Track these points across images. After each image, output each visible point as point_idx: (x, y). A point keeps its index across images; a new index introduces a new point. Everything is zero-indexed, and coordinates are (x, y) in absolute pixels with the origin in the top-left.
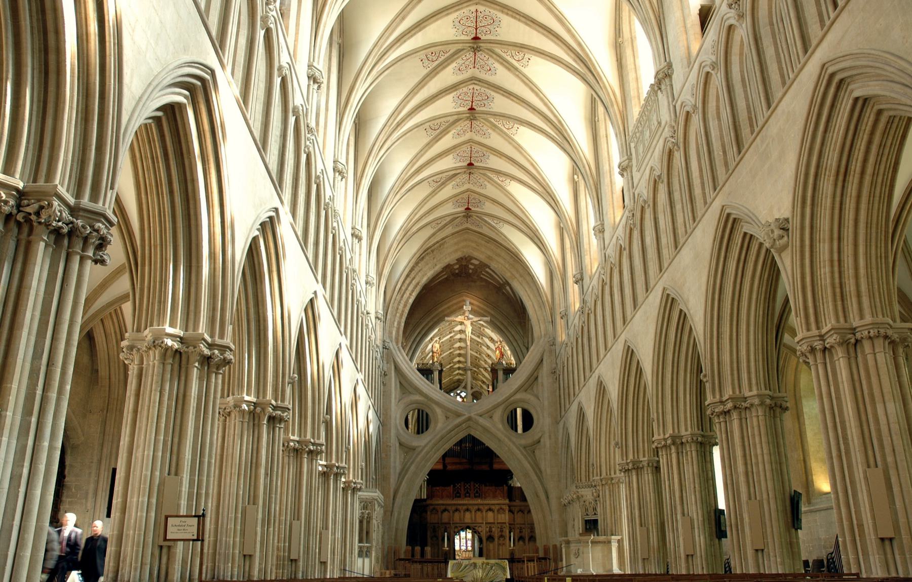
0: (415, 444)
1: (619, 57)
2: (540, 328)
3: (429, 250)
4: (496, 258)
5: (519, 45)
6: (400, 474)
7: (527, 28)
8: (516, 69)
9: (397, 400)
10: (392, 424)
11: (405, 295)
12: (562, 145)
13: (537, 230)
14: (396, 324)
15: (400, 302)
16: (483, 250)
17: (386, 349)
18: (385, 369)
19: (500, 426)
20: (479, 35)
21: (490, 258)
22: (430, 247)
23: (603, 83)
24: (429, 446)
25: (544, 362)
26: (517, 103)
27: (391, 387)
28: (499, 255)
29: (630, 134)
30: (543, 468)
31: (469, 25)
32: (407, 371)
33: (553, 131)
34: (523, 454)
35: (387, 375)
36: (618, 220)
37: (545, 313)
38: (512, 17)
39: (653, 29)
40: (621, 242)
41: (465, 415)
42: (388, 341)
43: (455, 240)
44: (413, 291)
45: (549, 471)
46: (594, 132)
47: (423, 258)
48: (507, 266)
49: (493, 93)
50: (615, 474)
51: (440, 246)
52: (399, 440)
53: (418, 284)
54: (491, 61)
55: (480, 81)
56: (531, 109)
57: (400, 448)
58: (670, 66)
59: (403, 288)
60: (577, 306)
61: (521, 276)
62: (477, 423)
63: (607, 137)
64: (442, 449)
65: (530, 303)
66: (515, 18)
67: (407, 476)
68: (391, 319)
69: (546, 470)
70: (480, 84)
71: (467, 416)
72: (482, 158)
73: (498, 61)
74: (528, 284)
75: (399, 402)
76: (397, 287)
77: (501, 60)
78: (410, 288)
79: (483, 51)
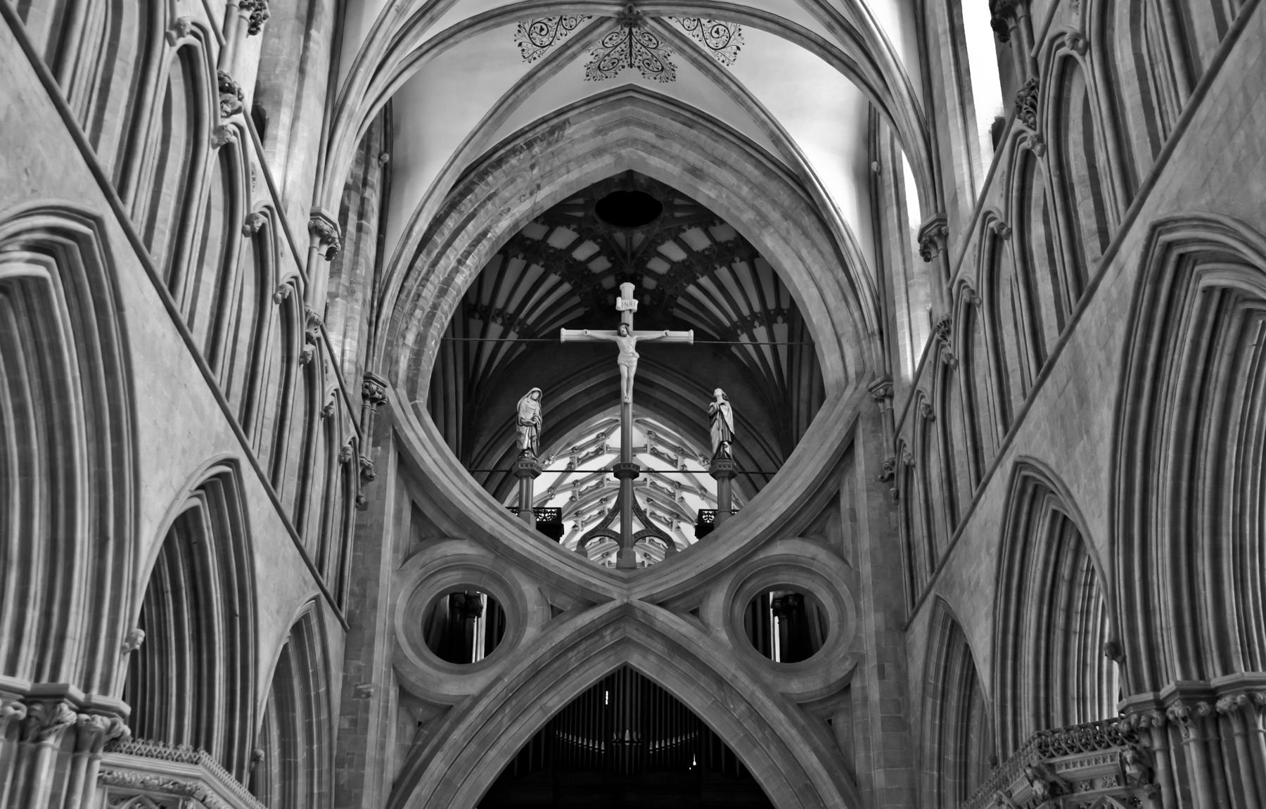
2: (843, 358)
3: (520, 141)
4: (713, 169)
6: (396, 785)
9: (401, 557)
11: (442, 262)
14: (410, 338)
15: (426, 279)
16: (676, 148)
17: (373, 400)
18: (367, 455)
19: (724, 636)
21: (695, 172)
22: (522, 133)
24: (493, 694)
25: (860, 451)
27: (382, 513)
28: (721, 163)
30: (860, 768)
34: (794, 723)
35: (371, 478)
37: (857, 315)
41: (614, 599)
42: (381, 378)
43: (596, 118)
44: (467, 254)
45: (879, 778)
47: (500, 162)
48: (745, 190)
50: (1227, 669)
51: (552, 131)
53: (484, 234)
59: (439, 240)
61: (786, 216)
62: (650, 628)
64: (537, 707)
65: (814, 291)
67: (417, 790)
68: (393, 320)
69: (870, 779)
71: (617, 603)
76: (416, 229)
78: (462, 243)
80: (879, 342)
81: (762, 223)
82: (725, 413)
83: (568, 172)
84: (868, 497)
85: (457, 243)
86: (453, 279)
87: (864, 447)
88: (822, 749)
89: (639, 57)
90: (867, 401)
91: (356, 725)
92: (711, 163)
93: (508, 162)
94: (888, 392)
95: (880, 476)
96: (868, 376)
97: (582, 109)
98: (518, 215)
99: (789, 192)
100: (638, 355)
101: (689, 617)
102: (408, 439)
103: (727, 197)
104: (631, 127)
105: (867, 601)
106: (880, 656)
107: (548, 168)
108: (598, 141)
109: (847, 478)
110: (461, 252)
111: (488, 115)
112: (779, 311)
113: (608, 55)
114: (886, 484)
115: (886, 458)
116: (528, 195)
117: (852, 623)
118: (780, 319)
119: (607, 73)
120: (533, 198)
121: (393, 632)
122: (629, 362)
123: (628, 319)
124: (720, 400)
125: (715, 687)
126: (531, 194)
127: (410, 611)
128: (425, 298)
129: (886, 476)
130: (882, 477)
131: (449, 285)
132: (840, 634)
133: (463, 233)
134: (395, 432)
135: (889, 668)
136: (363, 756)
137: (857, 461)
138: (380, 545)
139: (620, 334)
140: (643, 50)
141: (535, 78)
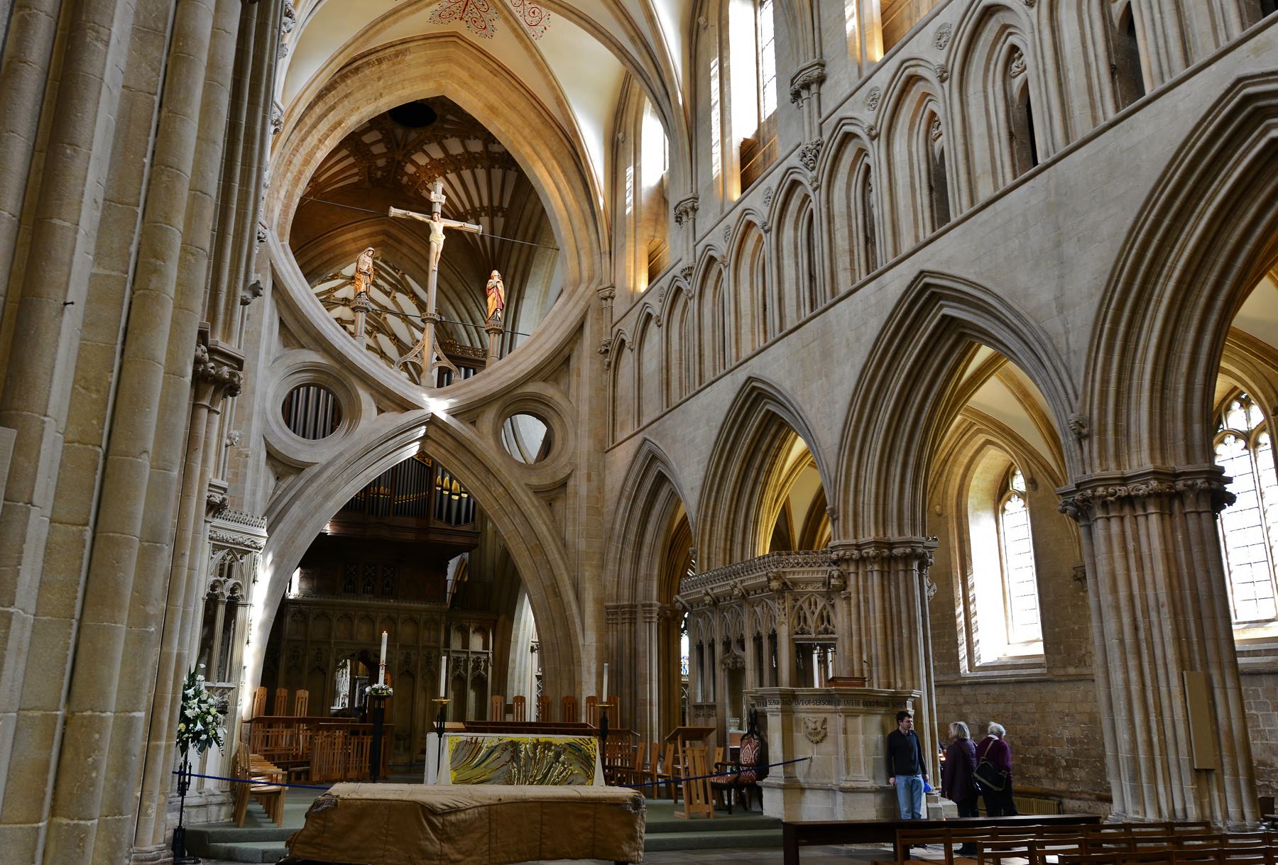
0: (304, 457)
3: (373, 57)
4: (507, 111)
10: (256, 408)
11: (309, 139)
14: (283, 193)
15: (296, 150)
16: (482, 89)
21: (492, 109)
22: (375, 51)
27: (261, 324)
30: (569, 536)
32: (299, 296)
37: (594, 237)
43: (428, 52)
44: (326, 136)
45: (582, 545)
47: (357, 70)
48: (527, 131)
51: (396, 56)
52: (268, 445)
53: (339, 123)
57: (267, 464)
59: (309, 121)
67: (281, 526)
75: (273, 362)
78: (323, 127)
80: (608, 259)
82: (500, 288)
83: (403, 88)
84: (591, 362)
85: (320, 126)
86: (315, 154)
88: (548, 522)
89: (470, 15)
90: (595, 297)
91: (237, 476)
93: (362, 72)
96: (596, 281)
97: (420, 43)
98: (364, 114)
99: (558, 140)
100: (444, 237)
101: (470, 426)
102: (281, 272)
103: (513, 133)
104: (452, 65)
105: (584, 430)
106: (589, 467)
107: (390, 83)
108: (426, 70)
109: (577, 346)
110: (321, 133)
111: (359, 34)
112: (500, 208)
113: (449, 8)
116: (373, 100)
117: (571, 443)
118: (500, 214)
119: (445, 21)
120: (376, 103)
121: (263, 413)
122: (438, 240)
123: (438, 208)
124: (496, 279)
125: (483, 475)
126: (376, 100)
127: (276, 397)
128: (295, 165)
129: (603, 350)
131: (311, 158)
132: (562, 449)
133: (325, 119)
134: (272, 265)
135: (594, 477)
136: (242, 498)
137: (584, 336)
138: (258, 348)
139: (432, 219)
140: (475, 10)
141: (399, 14)
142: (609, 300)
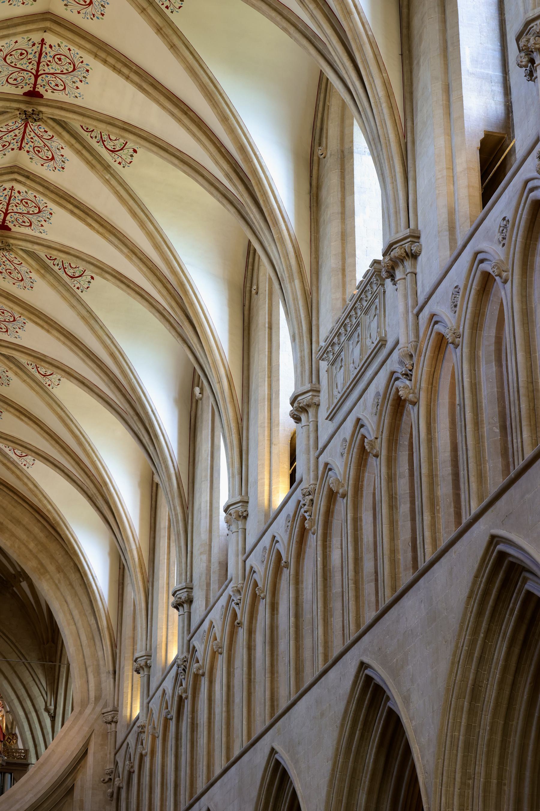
1: (314, 183)
4: (11, 526)
5: (120, 124)
7: (141, 96)
8: (107, 167)
12: (179, 329)
13: (106, 484)
20: (41, 90)
23: (280, 232)
25: (90, 758)
26: (98, 232)
28: (17, 522)
29: (322, 344)
31: (24, 67)
33: (166, 299)
36: (278, 501)
37: (100, 654)
38: (114, 68)
39: (390, 158)
40: (281, 547)
46: (246, 313)
48: (32, 545)
49: (51, 205)
54: (57, 142)
55: (28, 177)
56: (125, 250)
58: (415, 237)
60: (173, 653)
61: (59, 569)
63: (270, 328)
66: (120, 72)
70: (28, 182)
72: (10, 326)
73: (71, 146)
74: (73, 587)
77: (78, 146)
79: (45, 122)
80: (112, 680)
81: (42, 570)
87: (94, 756)
92: (9, 522)
94: (114, 720)
95: (102, 779)
114: (106, 785)
115: (108, 768)
129: (106, 780)
130: (104, 780)
142: (113, 724)
